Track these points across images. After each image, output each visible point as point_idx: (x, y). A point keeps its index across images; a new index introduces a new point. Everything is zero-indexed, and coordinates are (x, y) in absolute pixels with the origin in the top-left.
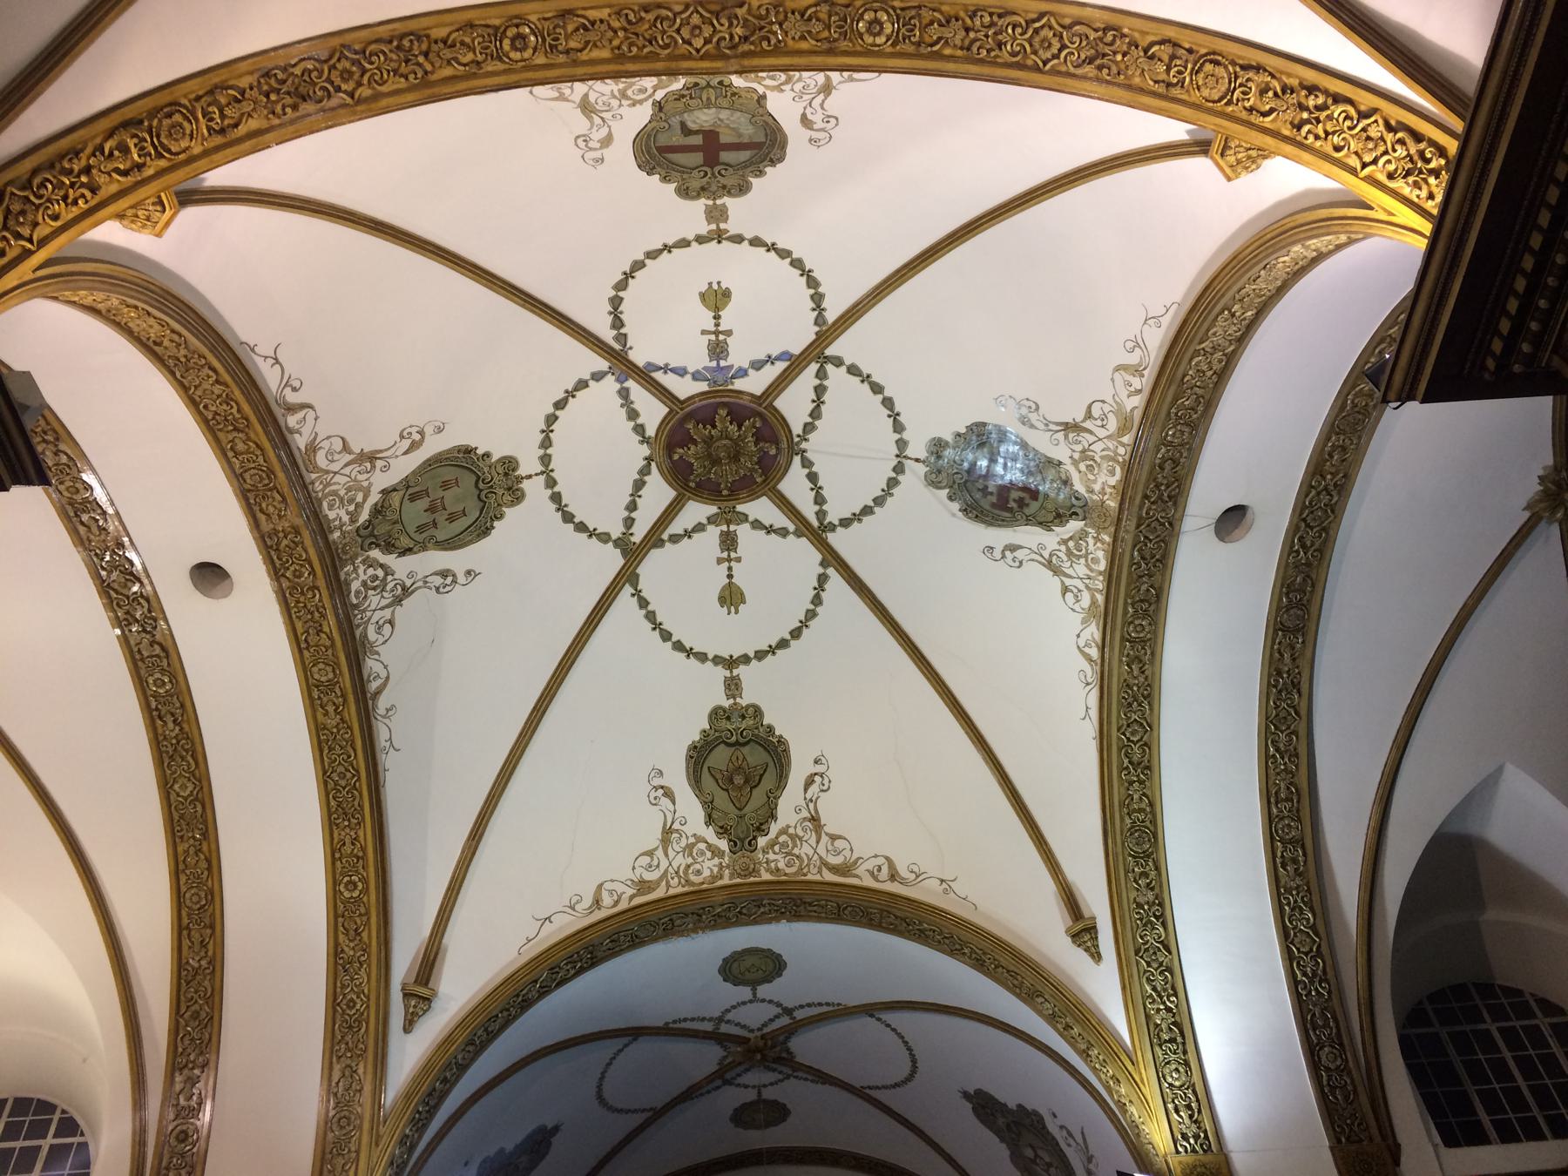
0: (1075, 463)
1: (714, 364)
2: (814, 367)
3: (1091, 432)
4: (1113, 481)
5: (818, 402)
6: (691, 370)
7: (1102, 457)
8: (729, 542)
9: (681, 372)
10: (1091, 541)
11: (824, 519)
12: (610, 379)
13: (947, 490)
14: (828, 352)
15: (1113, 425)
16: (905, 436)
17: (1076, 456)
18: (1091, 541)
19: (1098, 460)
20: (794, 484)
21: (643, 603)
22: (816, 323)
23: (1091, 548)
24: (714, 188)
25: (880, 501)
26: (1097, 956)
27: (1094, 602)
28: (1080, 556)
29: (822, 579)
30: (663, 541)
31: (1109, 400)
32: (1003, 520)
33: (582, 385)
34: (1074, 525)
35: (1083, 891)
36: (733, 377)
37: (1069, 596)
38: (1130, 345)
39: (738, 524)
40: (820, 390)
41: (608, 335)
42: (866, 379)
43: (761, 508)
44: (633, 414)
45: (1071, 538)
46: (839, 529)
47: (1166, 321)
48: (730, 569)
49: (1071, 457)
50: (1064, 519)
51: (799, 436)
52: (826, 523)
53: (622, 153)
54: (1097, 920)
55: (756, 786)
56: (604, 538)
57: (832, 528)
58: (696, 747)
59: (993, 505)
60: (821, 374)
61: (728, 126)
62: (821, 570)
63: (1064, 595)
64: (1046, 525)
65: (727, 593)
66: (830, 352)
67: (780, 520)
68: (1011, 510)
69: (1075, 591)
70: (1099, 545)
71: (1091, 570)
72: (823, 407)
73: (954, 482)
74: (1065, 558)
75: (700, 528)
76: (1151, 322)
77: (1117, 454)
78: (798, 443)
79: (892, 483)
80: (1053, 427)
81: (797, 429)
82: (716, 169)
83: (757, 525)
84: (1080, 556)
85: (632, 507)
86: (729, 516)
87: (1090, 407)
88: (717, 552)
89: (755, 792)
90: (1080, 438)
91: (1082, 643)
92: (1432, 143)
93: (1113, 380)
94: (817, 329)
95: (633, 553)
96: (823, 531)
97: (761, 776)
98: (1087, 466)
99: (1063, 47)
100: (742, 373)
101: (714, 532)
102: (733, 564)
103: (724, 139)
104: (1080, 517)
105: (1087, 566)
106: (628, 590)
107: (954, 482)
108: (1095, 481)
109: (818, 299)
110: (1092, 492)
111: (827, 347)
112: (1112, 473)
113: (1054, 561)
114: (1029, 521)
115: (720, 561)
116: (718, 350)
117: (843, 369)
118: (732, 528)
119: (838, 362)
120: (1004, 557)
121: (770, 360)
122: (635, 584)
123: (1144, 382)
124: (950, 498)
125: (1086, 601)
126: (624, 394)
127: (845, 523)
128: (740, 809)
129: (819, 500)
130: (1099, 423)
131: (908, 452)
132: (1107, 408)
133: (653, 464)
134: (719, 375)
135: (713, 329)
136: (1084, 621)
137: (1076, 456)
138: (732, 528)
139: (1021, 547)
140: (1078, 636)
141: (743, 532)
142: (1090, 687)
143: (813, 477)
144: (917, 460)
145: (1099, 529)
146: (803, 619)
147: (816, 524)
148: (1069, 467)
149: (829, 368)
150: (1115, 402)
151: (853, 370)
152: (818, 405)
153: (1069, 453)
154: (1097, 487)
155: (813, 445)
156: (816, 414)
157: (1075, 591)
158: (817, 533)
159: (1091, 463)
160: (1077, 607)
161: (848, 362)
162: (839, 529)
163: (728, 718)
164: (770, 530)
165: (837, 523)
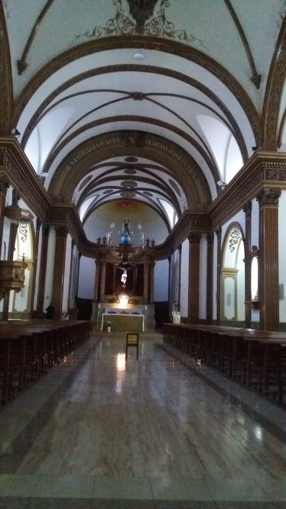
0: (153, 20)
4: (151, 31)
15: (168, 31)
18: (132, 27)
23: (129, 28)
26: (20, 73)
27: (112, 31)
31: (175, 29)
34: (135, 22)
37: (110, 22)
45: (130, 21)
49: (155, 18)
64: (131, 12)
74: (123, 18)
91: (98, 29)
93: (181, 30)
105: (123, 27)
110: (147, 26)
125: (112, 28)
136: (105, 29)
137: (156, 20)
140: (99, 27)
148: (152, 18)
154: (148, 27)
160: (108, 25)
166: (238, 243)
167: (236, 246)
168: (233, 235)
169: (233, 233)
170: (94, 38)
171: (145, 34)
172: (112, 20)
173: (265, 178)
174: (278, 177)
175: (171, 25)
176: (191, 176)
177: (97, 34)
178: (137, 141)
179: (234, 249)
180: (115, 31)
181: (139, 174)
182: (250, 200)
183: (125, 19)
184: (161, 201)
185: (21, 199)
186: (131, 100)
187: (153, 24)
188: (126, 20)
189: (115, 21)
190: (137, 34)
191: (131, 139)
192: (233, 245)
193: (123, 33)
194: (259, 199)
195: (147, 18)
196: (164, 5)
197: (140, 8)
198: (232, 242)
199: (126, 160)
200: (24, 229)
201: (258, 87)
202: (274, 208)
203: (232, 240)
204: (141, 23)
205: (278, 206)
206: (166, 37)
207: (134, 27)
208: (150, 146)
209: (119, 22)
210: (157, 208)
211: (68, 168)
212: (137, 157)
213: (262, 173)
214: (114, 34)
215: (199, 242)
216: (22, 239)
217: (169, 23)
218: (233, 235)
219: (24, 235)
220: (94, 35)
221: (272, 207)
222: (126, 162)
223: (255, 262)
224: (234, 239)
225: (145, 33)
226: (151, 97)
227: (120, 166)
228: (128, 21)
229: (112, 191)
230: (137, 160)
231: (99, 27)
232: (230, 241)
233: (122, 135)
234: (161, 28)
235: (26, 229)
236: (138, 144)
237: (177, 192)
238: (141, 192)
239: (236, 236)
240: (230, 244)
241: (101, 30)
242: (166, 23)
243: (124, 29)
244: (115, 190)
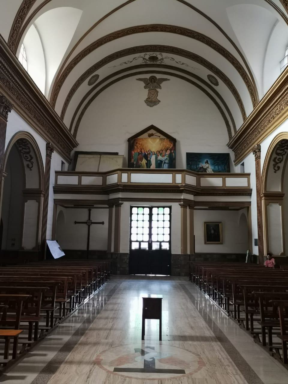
167: (281, 165)
169: (277, 149)
185: (12, 111)
192: (277, 163)
198: (277, 160)
200: (28, 155)
203: (275, 158)
216: (28, 166)
218: (279, 151)
219: (29, 161)
224: (278, 157)
232: (274, 160)
235: (30, 154)
240: (274, 163)
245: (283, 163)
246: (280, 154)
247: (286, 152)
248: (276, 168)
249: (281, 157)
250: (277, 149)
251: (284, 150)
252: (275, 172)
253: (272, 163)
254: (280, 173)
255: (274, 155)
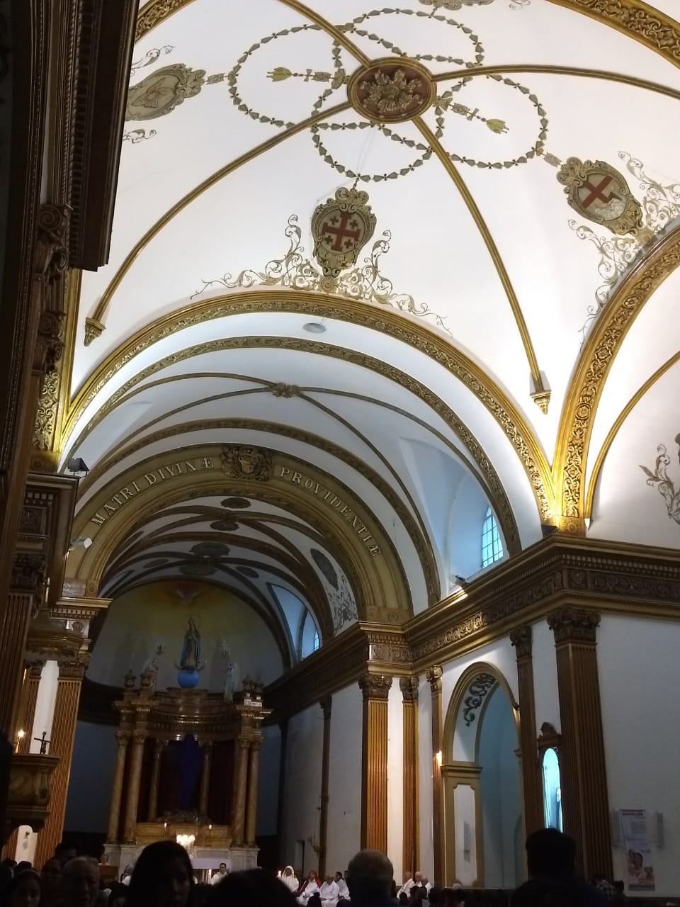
1: (452, 103)
2: (427, 145)
3: (375, 278)
4: (349, 291)
5: (403, 141)
6: (454, 93)
7: (361, 285)
8: (321, 77)
9: (456, 88)
10: (313, 278)
11: (321, 127)
12: (474, 61)
13: (334, 199)
14: (434, 154)
15: (381, 292)
16: (372, 181)
17: (360, 271)
18: (313, 278)
19: (359, 283)
20: (351, 116)
21: (295, 30)
22: (454, 155)
23: (309, 279)
24: (569, 171)
25: (329, 159)
26: (87, 343)
27: (275, 280)
28: (302, 272)
29: (280, 123)
30: (339, 45)
31: (393, 292)
32: (316, 229)
33: (479, 49)
34: (320, 270)
35: (109, 313)
36: (438, 108)
37: (275, 265)
38: (425, 306)
39: (332, 83)
40: (411, 144)
41: (505, 76)
42: (411, 168)
43: (340, 95)
44: (440, 59)
45: (311, 267)
46: (313, 134)
47: (441, 327)
48: (302, 75)
50: (322, 264)
51: (383, 126)
52: (319, 128)
53: (620, 167)
54: (104, 330)
55: (144, 105)
56: (359, 20)
57: (314, 130)
58: (181, 67)
59: (326, 224)
60: (420, 147)
61: (605, 208)
62: (286, 123)
63: (274, 261)
64: (316, 252)
65: (284, 72)
66: (434, 154)
67: (326, 105)
68: (323, 233)
69: (279, 269)
70: (311, 283)
71: (295, 278)
72: (399, 142)
73: (340, 204)
74: (299, 263)
75: (338, 64)
76: (439, 319)
77: (365, 293)
78: (379, 125)
79: (341, 169)
80: (374, 259)
81: (387, 126)
82: (582, 184)
83: (328, 93)
84: (302, 272)
85: (373, 37)
86: (340, 79)
87: (387, 280)
88: (317, 69)
89: (143, 108)
90: (369, 274)
91: (248, 273)
92: (579, 493)
93: (404, 294)
94: (451, 154)
95: (338, 33)
96: (313, 126)
97: (151, 107)
98: (355, 277)
99: (600, 360)
100: (438, 112)
101: (332, 70)
102: (304, 77)
103: (597, 201)
104: (326, 274)
105: (297, 276)
106: (310, 23)
107: (340, 204)
108: (347, 281)
109: (471, 163)
110: (341, 280)
111: (437, 153)
112: (353, 291)
113: (294, 256)
114: (318, 243)
115: (309, 71)
116: (460, 109)
117: (421, 158)
118: (331, 80)
119: (426, 157)
120: (292, 226)
121: (440, 127)
122: (312, 27)
123: (406, 314)
124: (329, 201)
125: (275, 275)
126: (460, 62)
127: (316, 139)
128: (132, 104)
129: (335, 127)
130: (380, 285)
131: (360, 181)
132: (389, 289)
133: (399, 56)
134: (444, 102)
135: (477, 114)
136: (262, 275)
137: (360, 271)
138: (331, 80)
139: (300, 237)
140: (251, 271)
141: (327, 85)
142: (224, 282)
143: (353, 126)
144: (355, 185)
145: (321, 283)
146: (238, 96)
147: (319, 123)
148: (353, 267)
149: (424, 152)
150: (393, 295)
151: (418, 163)
152: (401, 140)
153: (361, 267)
154: (344, 283)
155: (375, 133)
156: (396, 137)
157: (279, 269)
158: (314, 121)
159: (357, 280)
161: (414, 148)
162: (313, 134)
163: (195, 80)
164: (322, 99)
165: (317, 134)
166: (482, 705)
167: (477, 712)
168: (475, 689)
170: (238, 290)
171: (337, 293)
172: (278, 263)
173: (566, 584)
174: (589, 585)
175: (385, 283)
176: (367, 549)
177: (245, 282)
178: (255, 468)
179: (473, 717)
180: (280, 283)
181: (244, 531)
182: (530, 621)
183: (305, 263)
184: (275, 589)
186: (267, 398)
187: (354, 279)
188: (304, 265)
189: (283, 264)
190: (323, 292)
191: (243, 462)
192: (471, 708)
193: (294, 287)
194: (555, 625)
195: (344, 266)
196: (379, 249)
197: (333, 248)
199: (223, 503)
201: (545, 410)
202: (589, 647)
203: (470, 698)
204: (331, 272)
205: (595, 644)
206: (374, 303)
207: (318, 279)
208: (281, 479)
209: (290, 266)
210: (258, 601)
211: (101, 518)
212: (249, 500)
213: (558, 576)
214: (278, 287)
215: (385, 697)
217: (383, 280)
218: (475, 689)
220: (240, 285)
221: (585, 647)
222: (223, 507)
223: (551, 761)
225: (337, 291)
226: (306, 393)
227: (207, 513)
228: (308, 267)
229: (167, 561)
230: (248, 504)
231: (251, 271)
232: (467, 702)
233: (225, 454)
234: (368, 285)
236: (259, 474)
237: (325, 573)
238: (233, 567)
239: (479, 689)
240: (467, 707)
241: (254, 277)
242: (378, 279)
243: (297, 280)
244: (171, 560)
245: (480, 709)
246: (477, 692)
247: (486, 692)
248: (468, 717)
249: (478, 698)
250: (473, 685)
251: (483, 687)
252: (468, 725)
253: (463, 706)
254: (474, 724)
255: (468, 694)
